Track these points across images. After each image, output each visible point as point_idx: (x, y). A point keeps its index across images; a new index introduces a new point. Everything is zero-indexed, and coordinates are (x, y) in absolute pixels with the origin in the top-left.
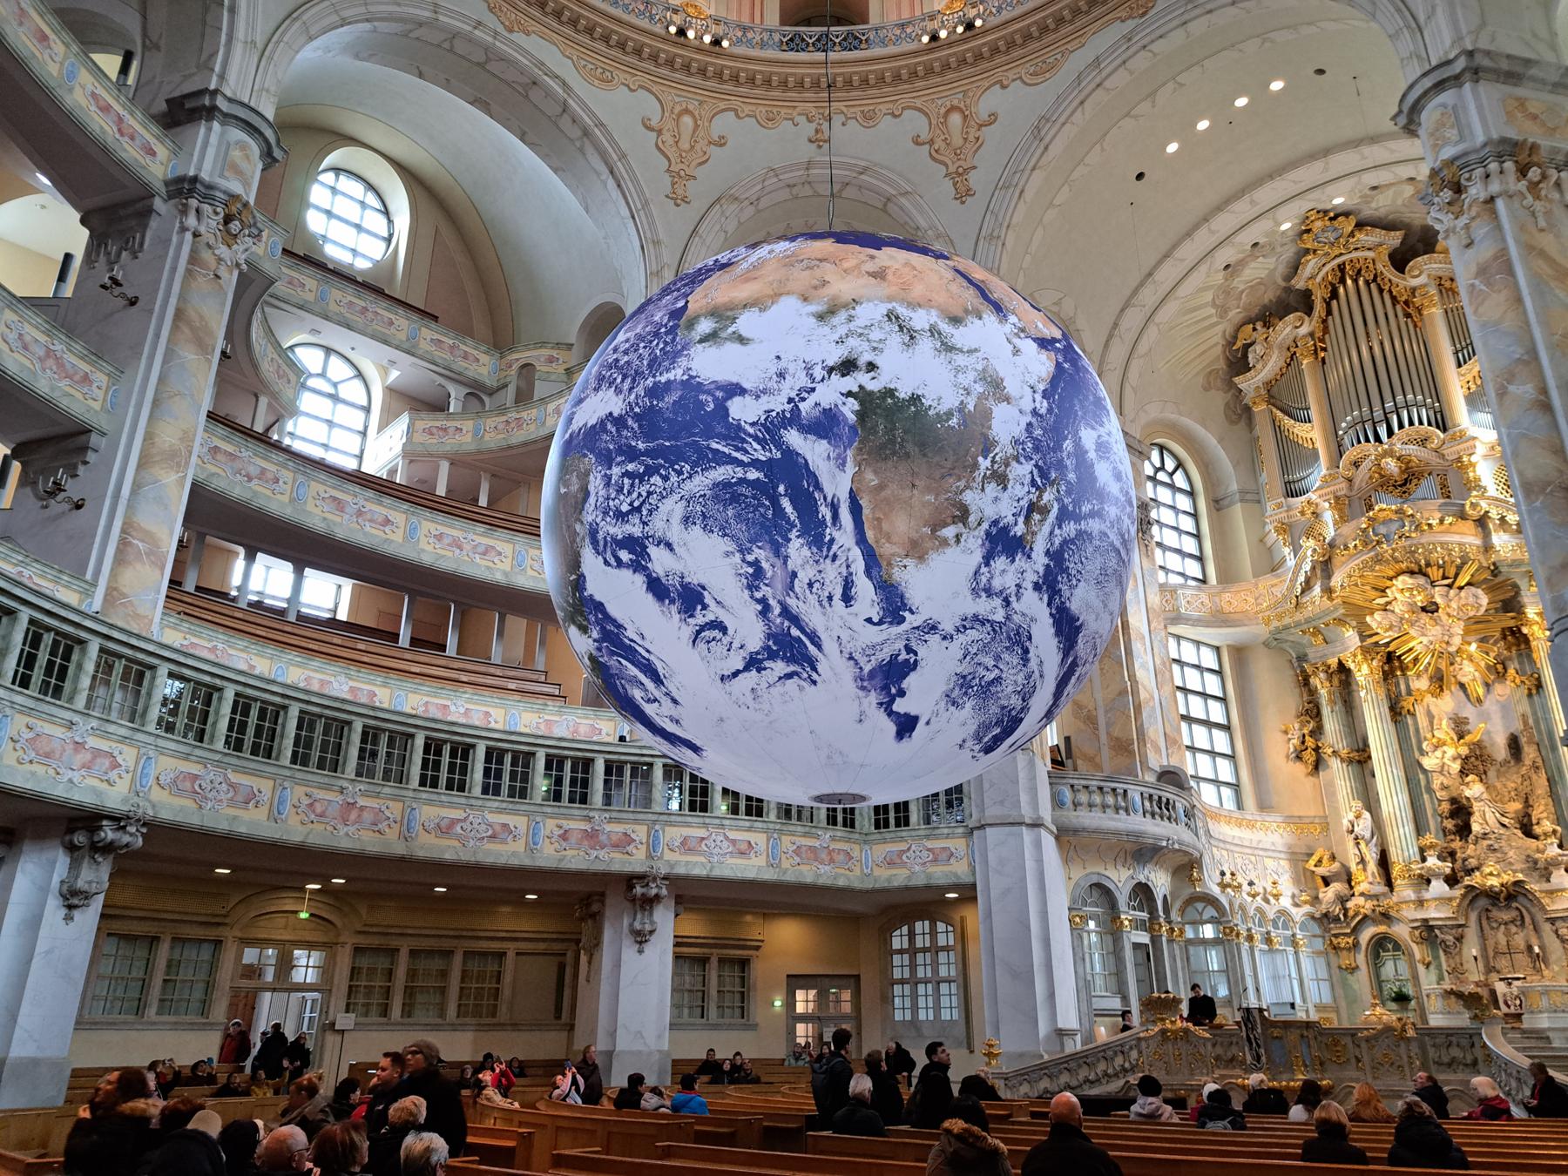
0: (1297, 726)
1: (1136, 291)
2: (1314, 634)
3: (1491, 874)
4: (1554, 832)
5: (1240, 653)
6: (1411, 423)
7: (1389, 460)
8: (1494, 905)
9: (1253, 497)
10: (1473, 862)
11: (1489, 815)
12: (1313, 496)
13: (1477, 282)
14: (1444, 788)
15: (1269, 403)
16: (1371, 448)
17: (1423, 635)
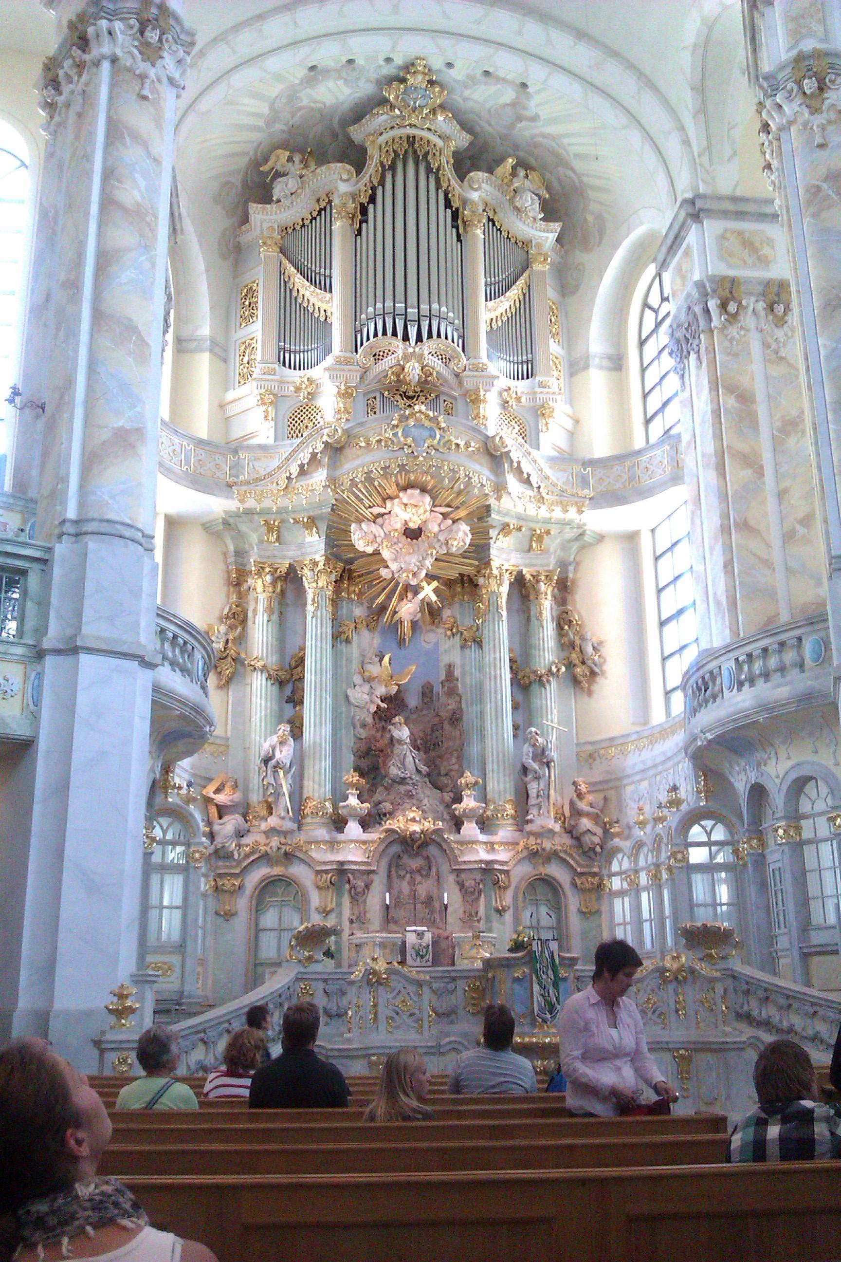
0: (223, 628)
1: (236, 28)
2: (270, 529)
3: (413, 820)
4: (476, 783)
5: (173, 524)
6: (439, 336)
7: (417, 365)
8: (407, 851)
9: (220, 351)
10: (387, 806)
11: (409, 760)
12: (318, 373)
13: (825, 186)
14: (364, 726)
15: (282, 251)
16: (398, 344)
17: (395, 560)
